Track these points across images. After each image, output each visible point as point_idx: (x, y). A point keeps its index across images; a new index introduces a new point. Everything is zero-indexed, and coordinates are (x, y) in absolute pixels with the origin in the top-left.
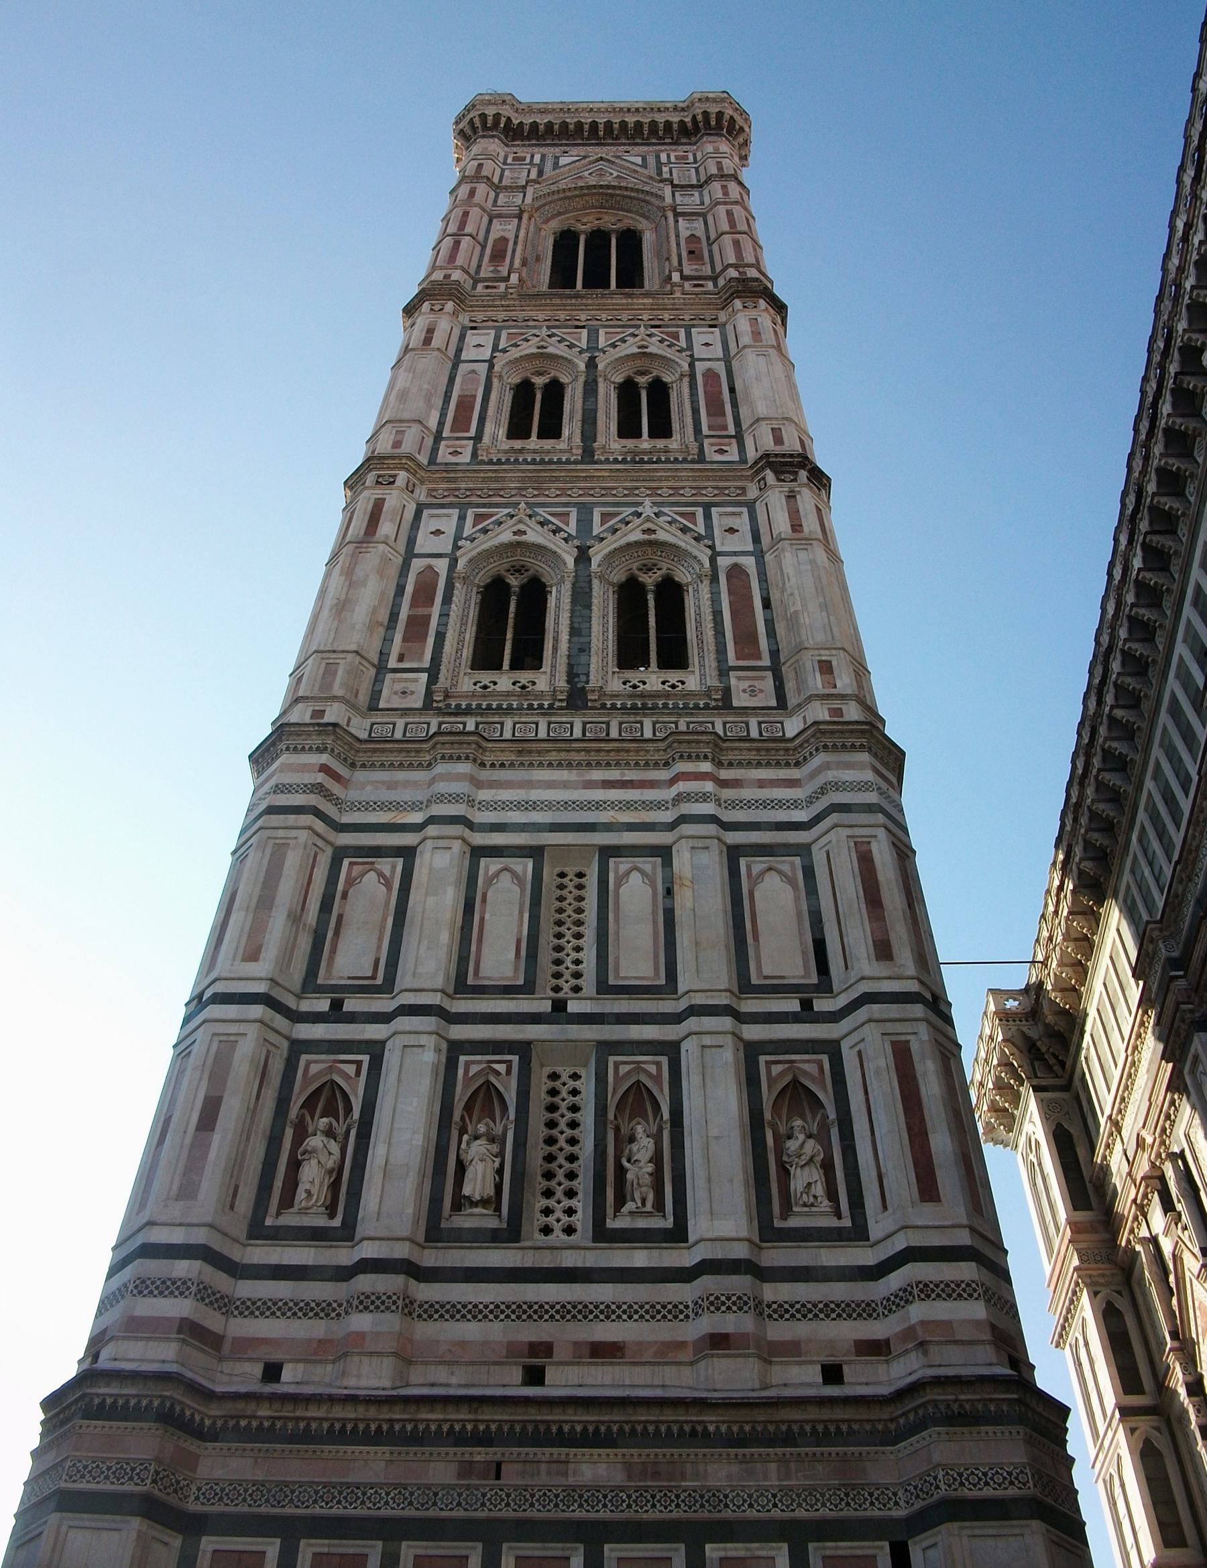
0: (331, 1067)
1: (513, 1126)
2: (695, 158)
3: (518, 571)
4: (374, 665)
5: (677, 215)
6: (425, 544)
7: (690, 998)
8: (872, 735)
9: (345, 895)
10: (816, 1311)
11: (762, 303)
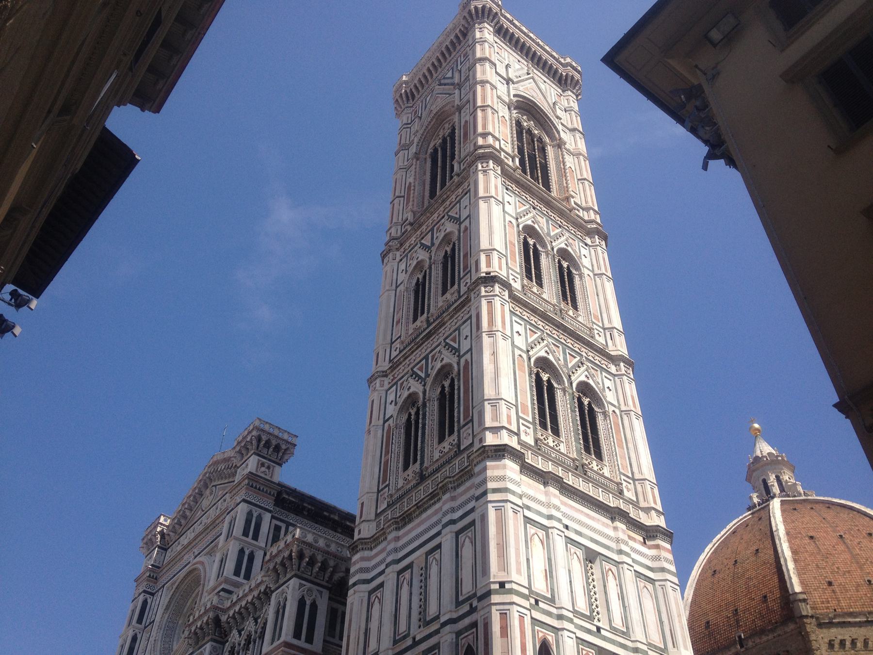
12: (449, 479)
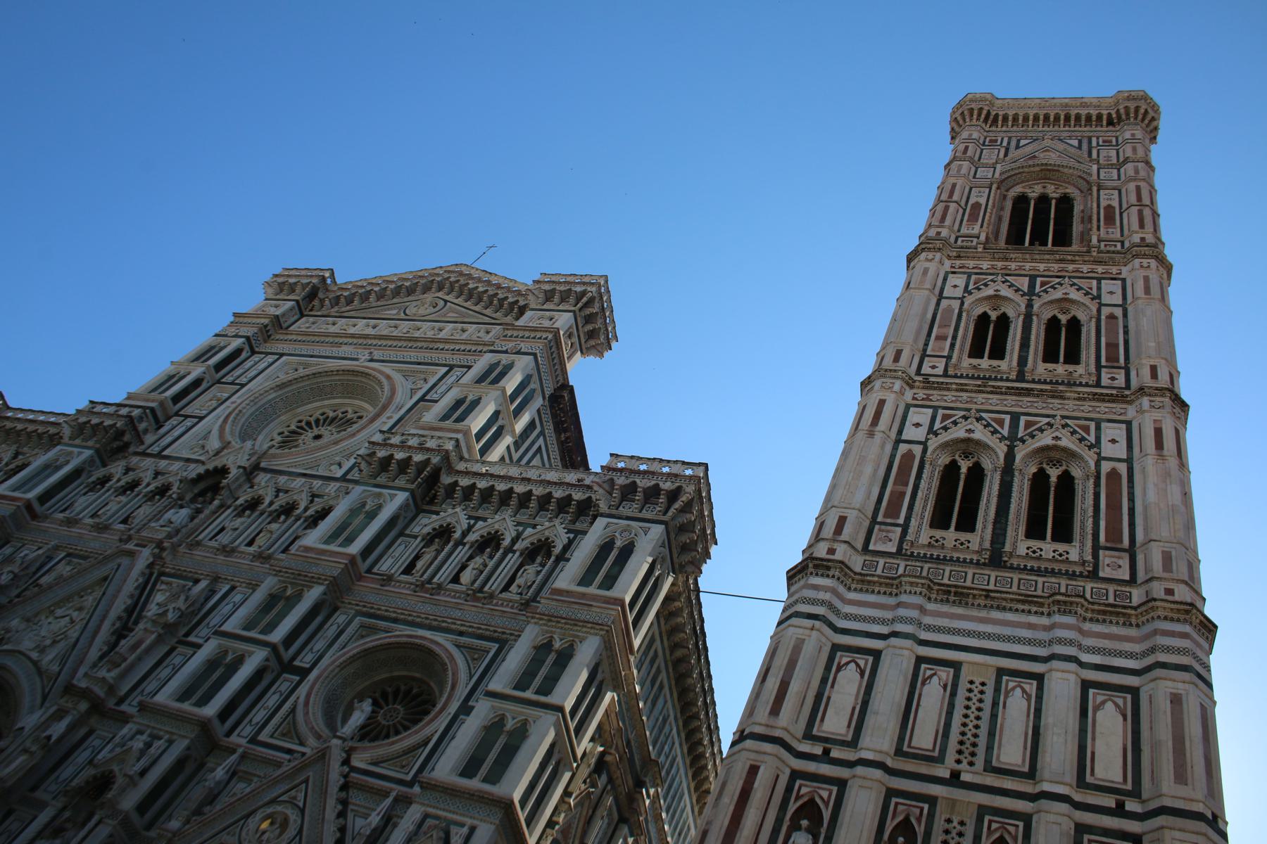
2: (1117, 141)
3: (967, 457)
5: (1098, 191)
6: (909, 434)
12: (1082, 600)
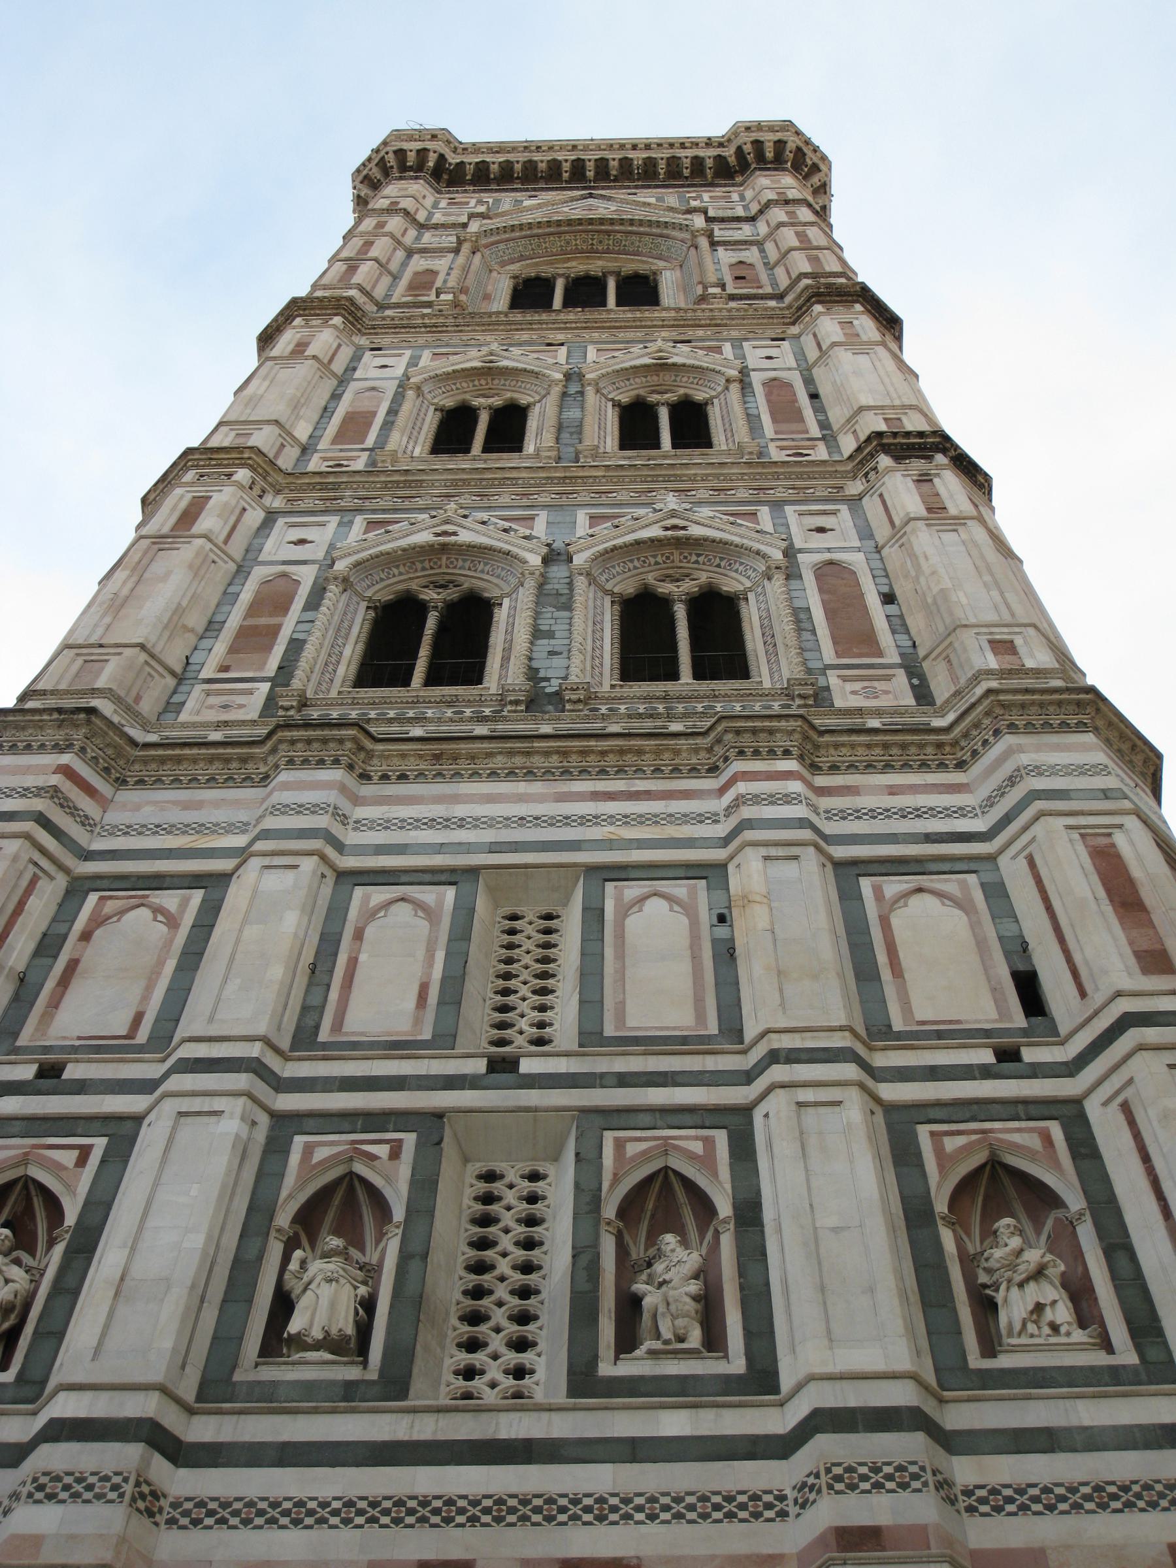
0: (26, 1154)
1: (400, 1231)
2: (742, 198)
4: (173, 673)
5: (714, 244)
7: (769, 1041)
8: (1098, 710)
9: (86, 936)
10: (1077, 1498)
11: (858, 307)
